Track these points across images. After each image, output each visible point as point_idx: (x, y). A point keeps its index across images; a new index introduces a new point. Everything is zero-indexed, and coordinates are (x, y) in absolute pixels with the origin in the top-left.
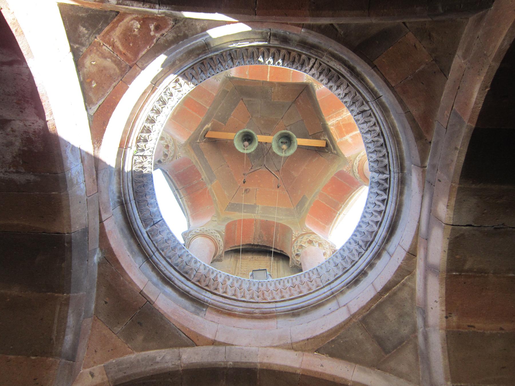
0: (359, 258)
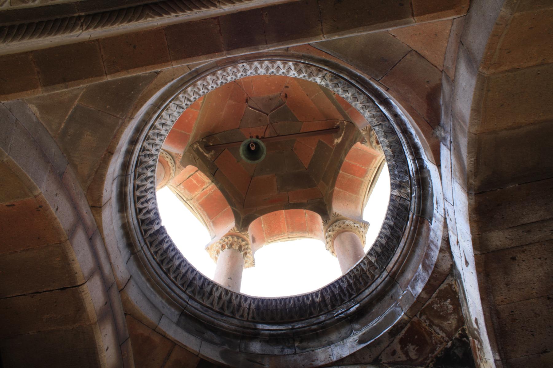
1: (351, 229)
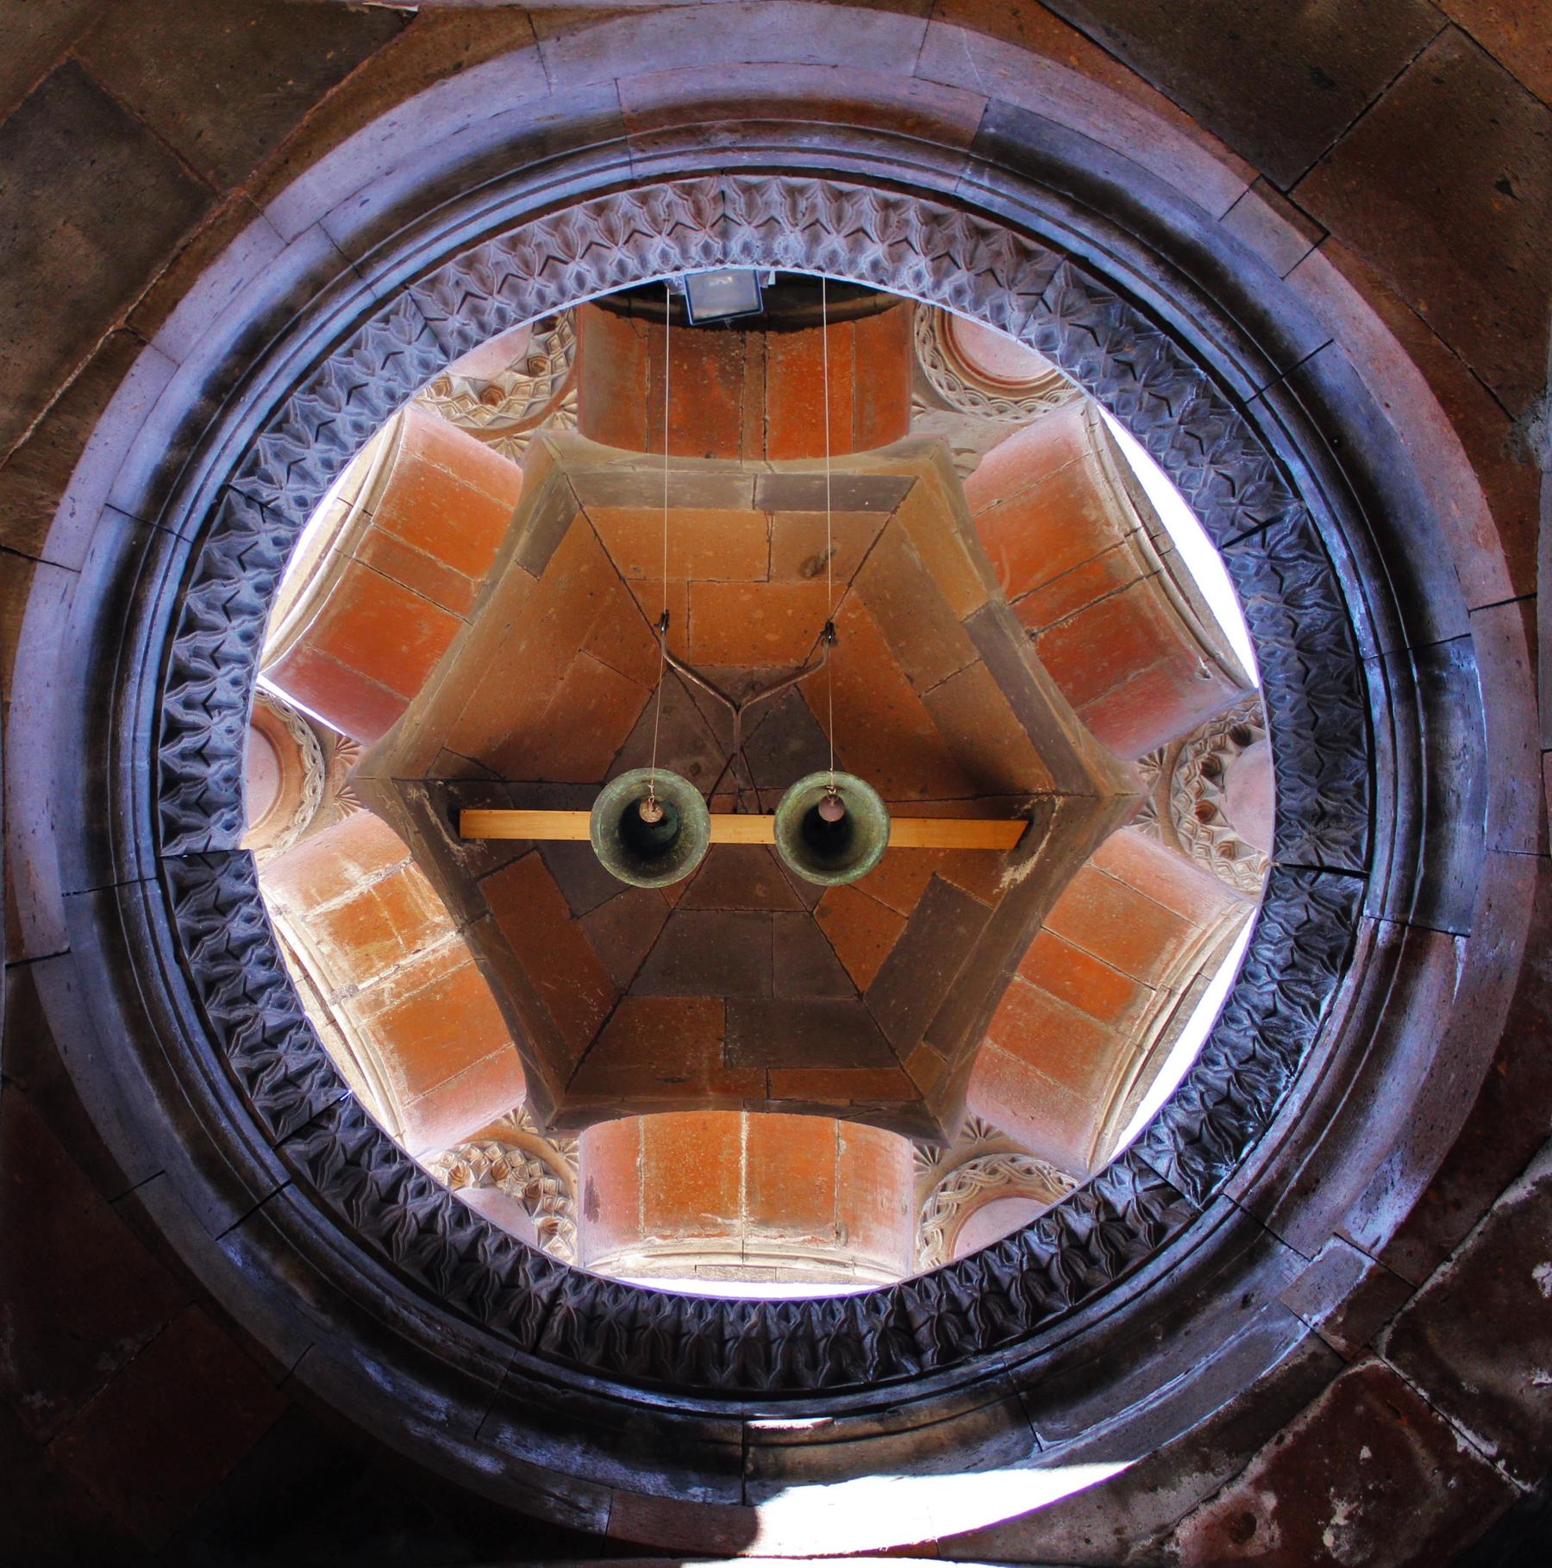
0: (255, 447)
1: (1040, 1190)
